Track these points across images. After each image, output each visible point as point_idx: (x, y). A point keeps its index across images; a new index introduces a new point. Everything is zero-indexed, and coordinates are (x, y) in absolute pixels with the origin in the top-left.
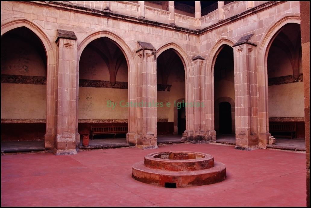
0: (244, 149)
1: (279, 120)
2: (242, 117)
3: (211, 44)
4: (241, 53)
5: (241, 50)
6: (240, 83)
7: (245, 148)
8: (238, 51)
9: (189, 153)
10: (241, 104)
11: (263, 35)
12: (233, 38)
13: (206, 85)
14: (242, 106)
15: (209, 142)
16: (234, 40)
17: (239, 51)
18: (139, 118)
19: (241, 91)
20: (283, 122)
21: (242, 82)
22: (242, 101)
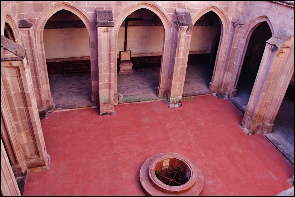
0: (110, 114)
1: (78, 59)
2: (106, 90)
3: (44, 6)
4: (106, 34)
5: (107, 32)
6: (104, 61)
7: (111, 113)
8: (102, 32)
9: (159, 161)
10: (104, 80)
11: (120, 13)
12: (82, 8)
13: (38, 54)
14: (105, 81)
15: (51, 111)
16: (83, 9)
17: (104, 32)
18: (26, 143)
19: (104, 69)
20: (83, 60)
21: (106, 61)
22: (106, 77)
